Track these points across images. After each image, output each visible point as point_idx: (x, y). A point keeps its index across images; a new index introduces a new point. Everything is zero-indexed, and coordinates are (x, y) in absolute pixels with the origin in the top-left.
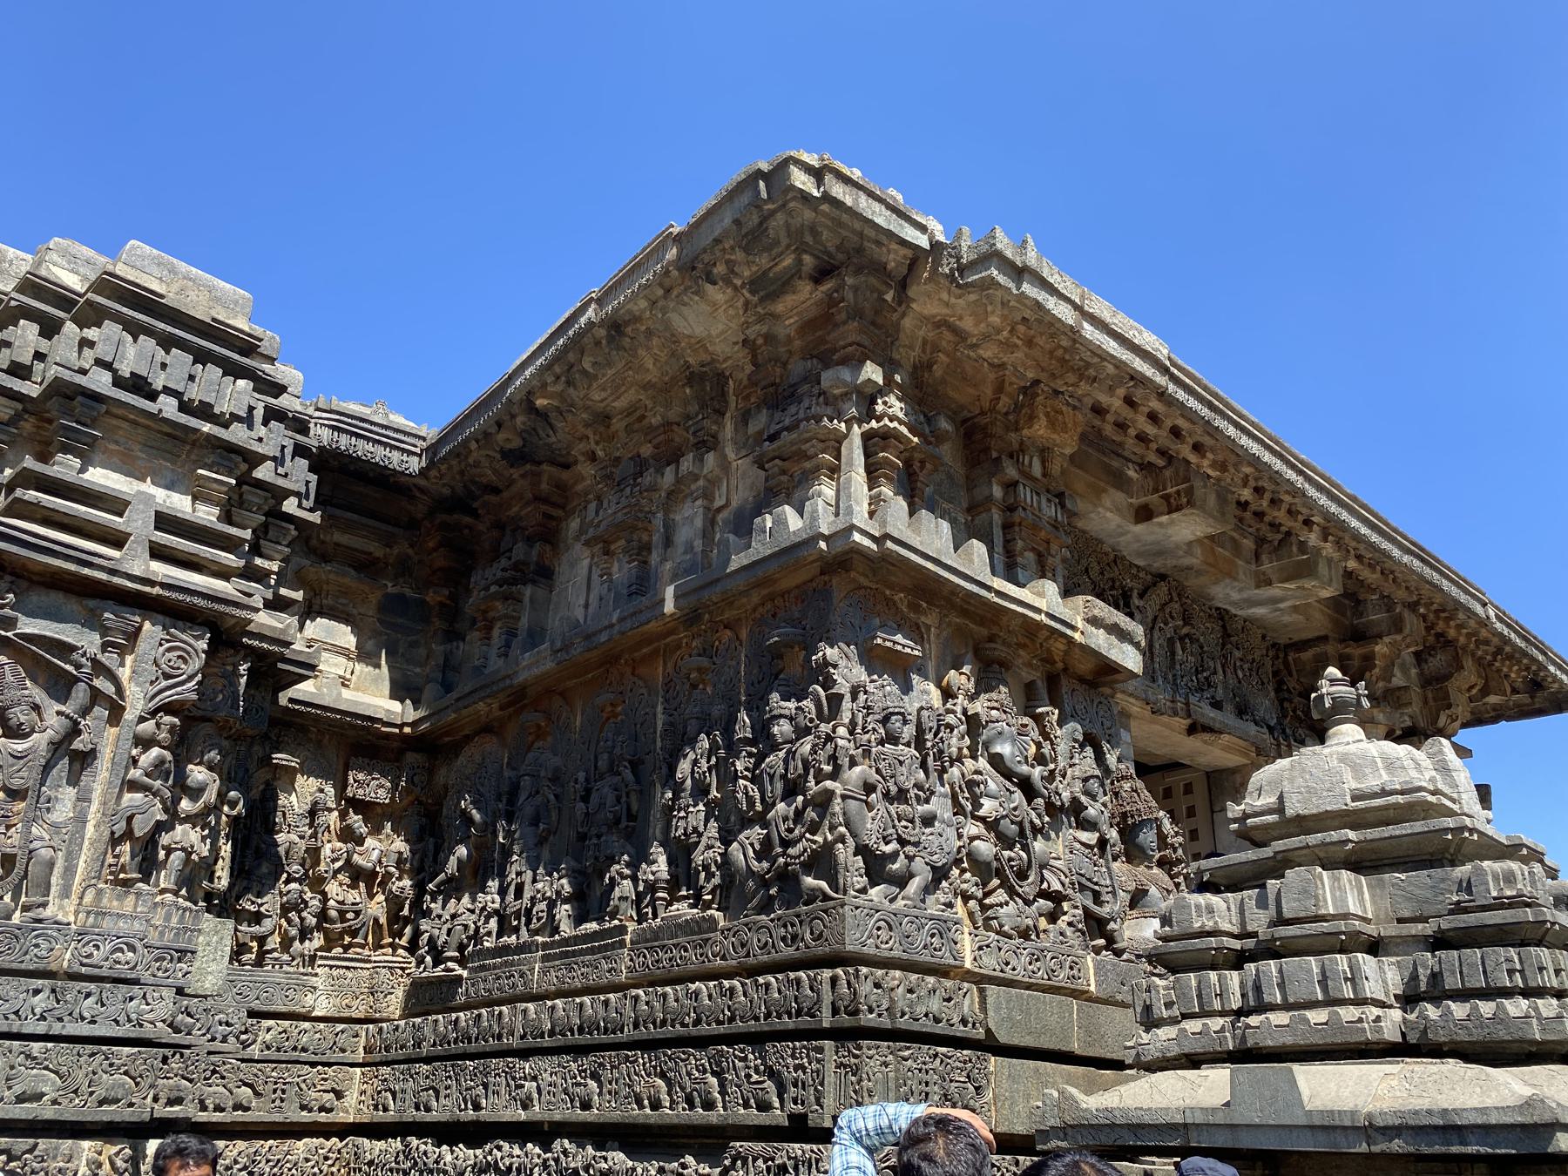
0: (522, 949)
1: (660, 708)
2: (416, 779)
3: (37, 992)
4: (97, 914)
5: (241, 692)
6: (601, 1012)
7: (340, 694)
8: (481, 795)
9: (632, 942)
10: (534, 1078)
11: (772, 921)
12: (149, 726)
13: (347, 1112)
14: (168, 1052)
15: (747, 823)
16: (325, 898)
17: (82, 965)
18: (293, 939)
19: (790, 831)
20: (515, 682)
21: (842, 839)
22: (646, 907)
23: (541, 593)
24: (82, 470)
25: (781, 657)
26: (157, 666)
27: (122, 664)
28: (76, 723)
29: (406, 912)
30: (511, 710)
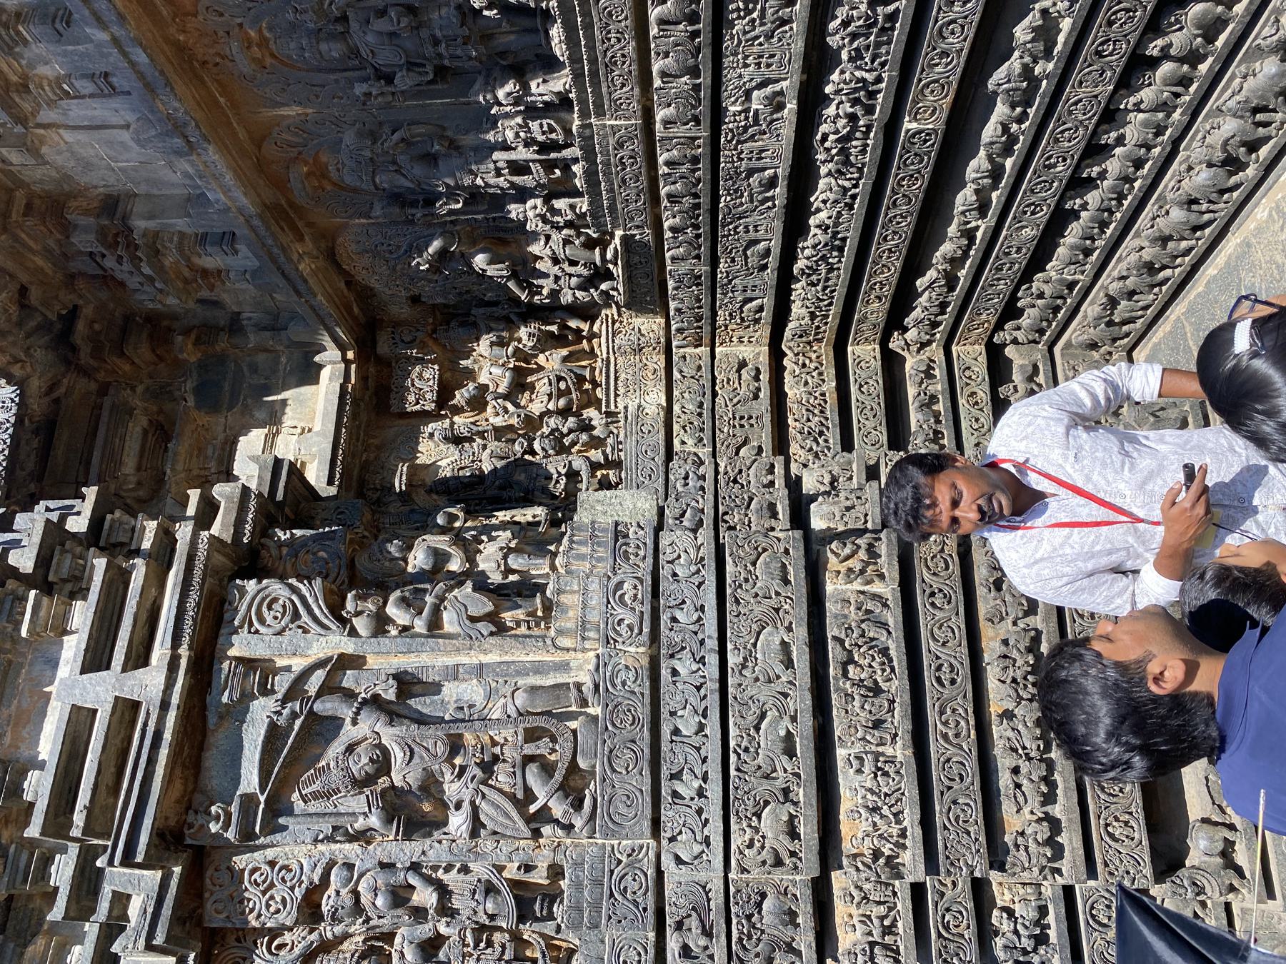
0: (589, 154)
2: (408, 339)
3: (675, 673)
4: (584, 629)
5: (312, 532)
7: (318, 434)
8: (410, 247)
10: (748, 94)
12: (361, 624)
13: (758, 354)
14: (723, 527)
16: (548, 413)
17: (641, 632)
18: (592, 437)
20: (252, 210)
23: (139, 207)
24: (41, 766)
26: (283, 630)
27: (288, 669)
28: (365, 702)
29: (554, 328)
30: (300, 224)
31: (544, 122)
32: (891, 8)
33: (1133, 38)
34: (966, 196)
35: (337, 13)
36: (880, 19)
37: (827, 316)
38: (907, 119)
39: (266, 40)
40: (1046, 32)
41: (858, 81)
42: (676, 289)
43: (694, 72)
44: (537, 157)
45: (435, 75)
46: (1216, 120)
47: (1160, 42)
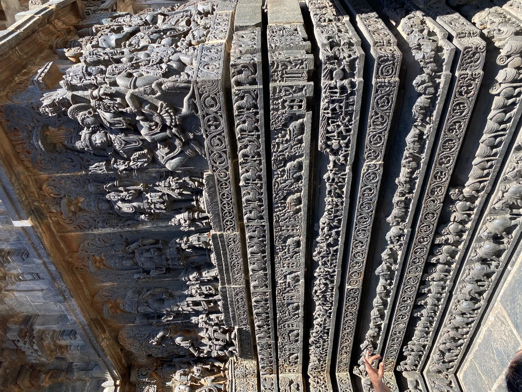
0: (225, 297)
1: (96, 232)
2: (144, 374)
6: (256, 240)
9: (220, 230)
10: (285, 277)
11: (207, 136)
13: (298, 377)
15: (154, 161)
19: (157, 124)
20: (86, 322)
21: (160, 85)
22: (202, 224)
23: (39, 320)
25: (55, 145)
29: (208, 367)
30: (105, 326)
31: (207, 286)
32: (335, 248)
33: (425, 257)
34: (374, 313)
35: (131, 251)
36: (332, 251)
37: (325, 361)
38: (347, 285)
39: (103, 260)
40: (393, 255)
41: (326, 272)
42: (261, 350)
43: (265, 269)
44: (204, 299)
45: (166, 270)
46: (464, 284)
47: (435, 258)
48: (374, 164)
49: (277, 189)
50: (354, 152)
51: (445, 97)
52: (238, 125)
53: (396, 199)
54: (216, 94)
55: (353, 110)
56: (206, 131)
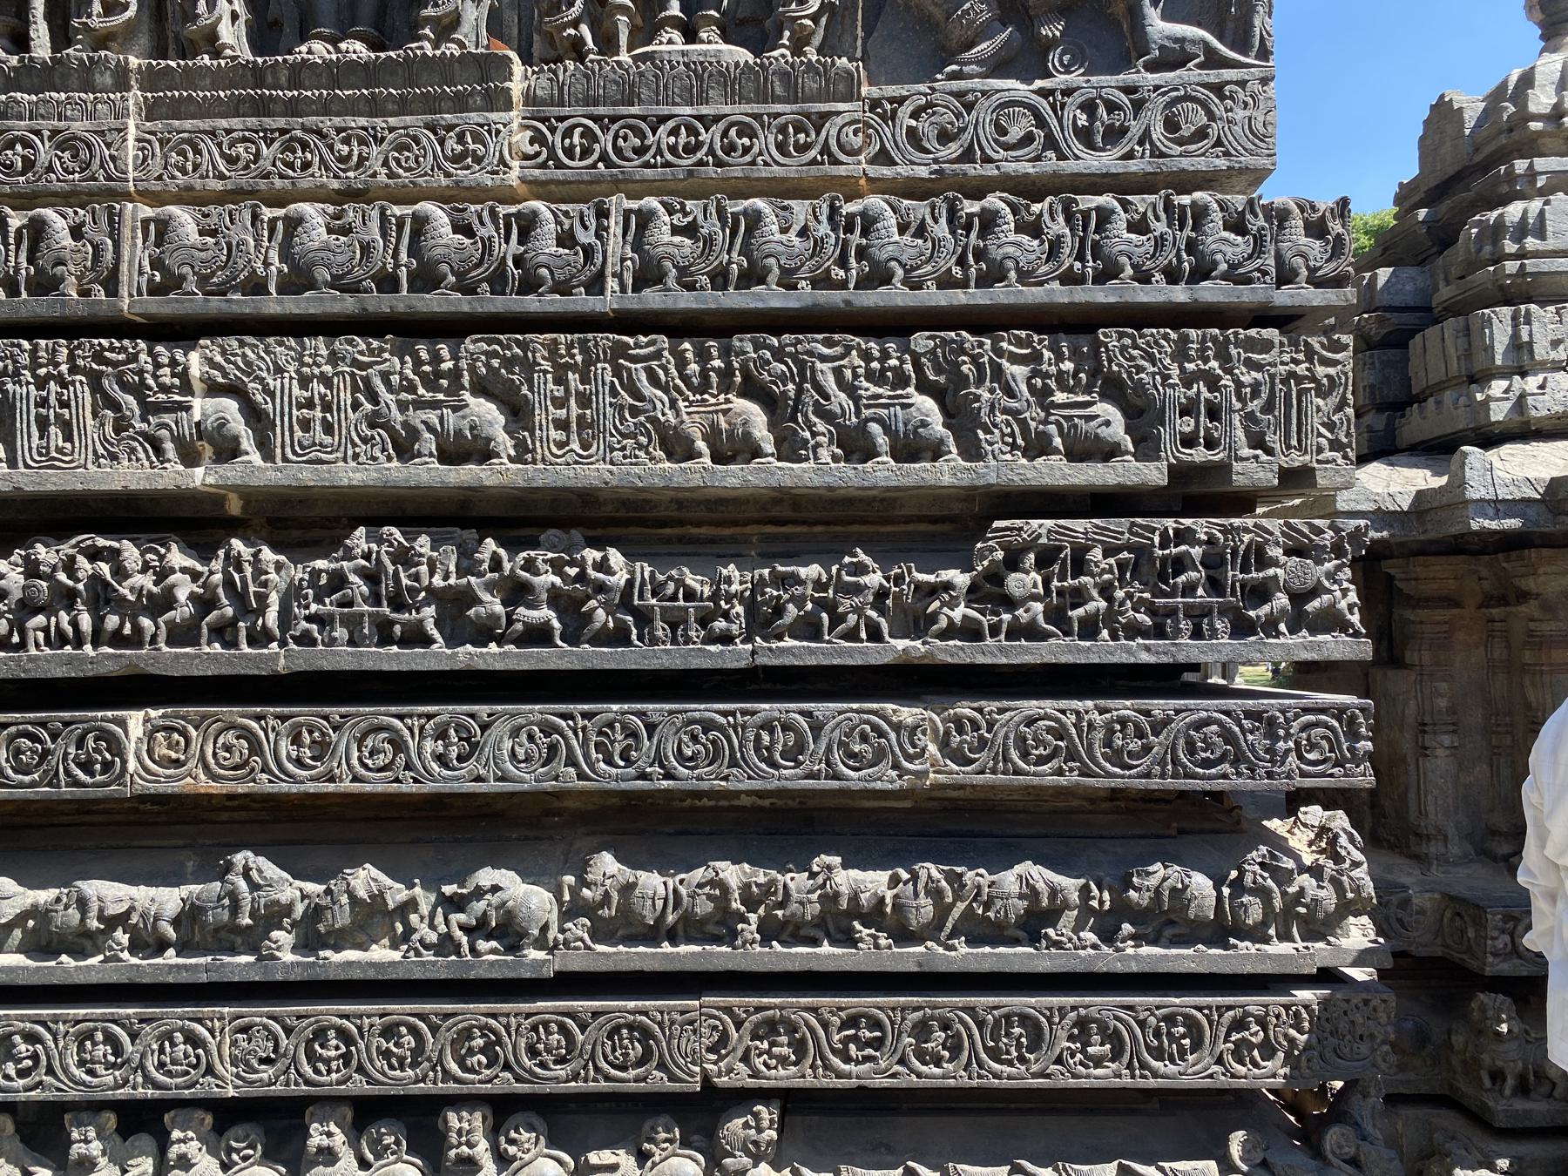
9: (530, 99)
22: (575, 24)
32: (432, 629)
38: (153, 713)
41: (262, 599)
43: (298, 279)
47: (339, 1138)
48: (924, 750)
49: (810, 353)
50: (989, 660)
51: (1228, 970)
52: (1125, 205)
53: (732, 873)
54: (1219, 143)
55: (1177, 632)
56: (1068, 92)
